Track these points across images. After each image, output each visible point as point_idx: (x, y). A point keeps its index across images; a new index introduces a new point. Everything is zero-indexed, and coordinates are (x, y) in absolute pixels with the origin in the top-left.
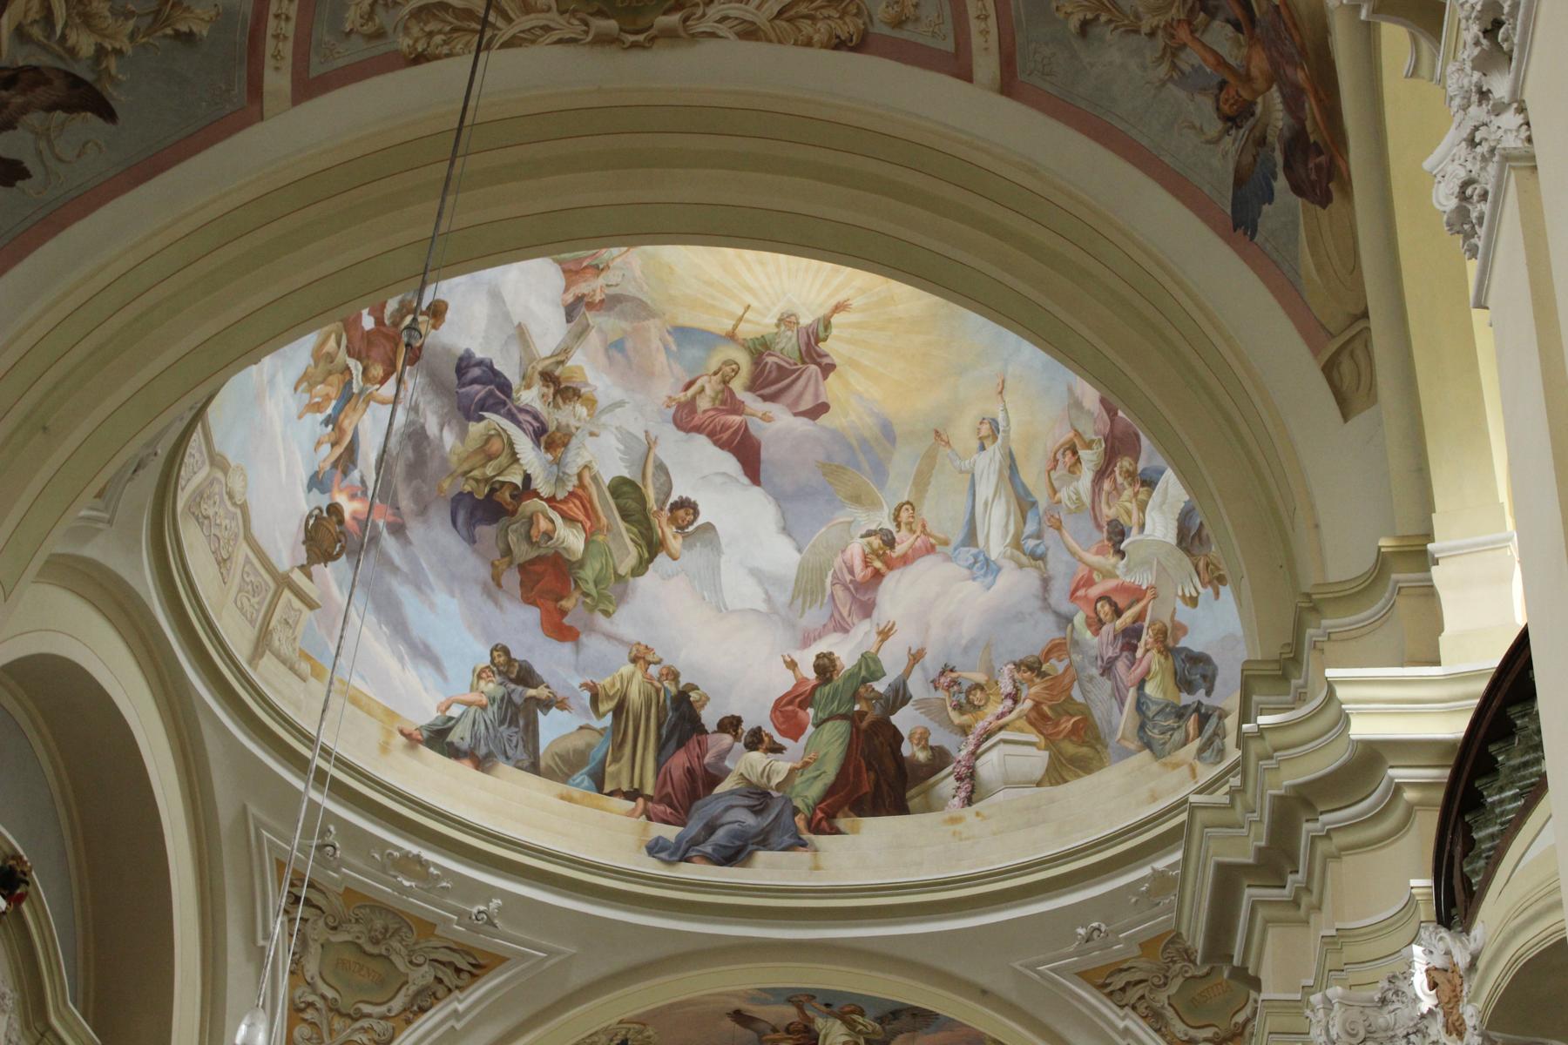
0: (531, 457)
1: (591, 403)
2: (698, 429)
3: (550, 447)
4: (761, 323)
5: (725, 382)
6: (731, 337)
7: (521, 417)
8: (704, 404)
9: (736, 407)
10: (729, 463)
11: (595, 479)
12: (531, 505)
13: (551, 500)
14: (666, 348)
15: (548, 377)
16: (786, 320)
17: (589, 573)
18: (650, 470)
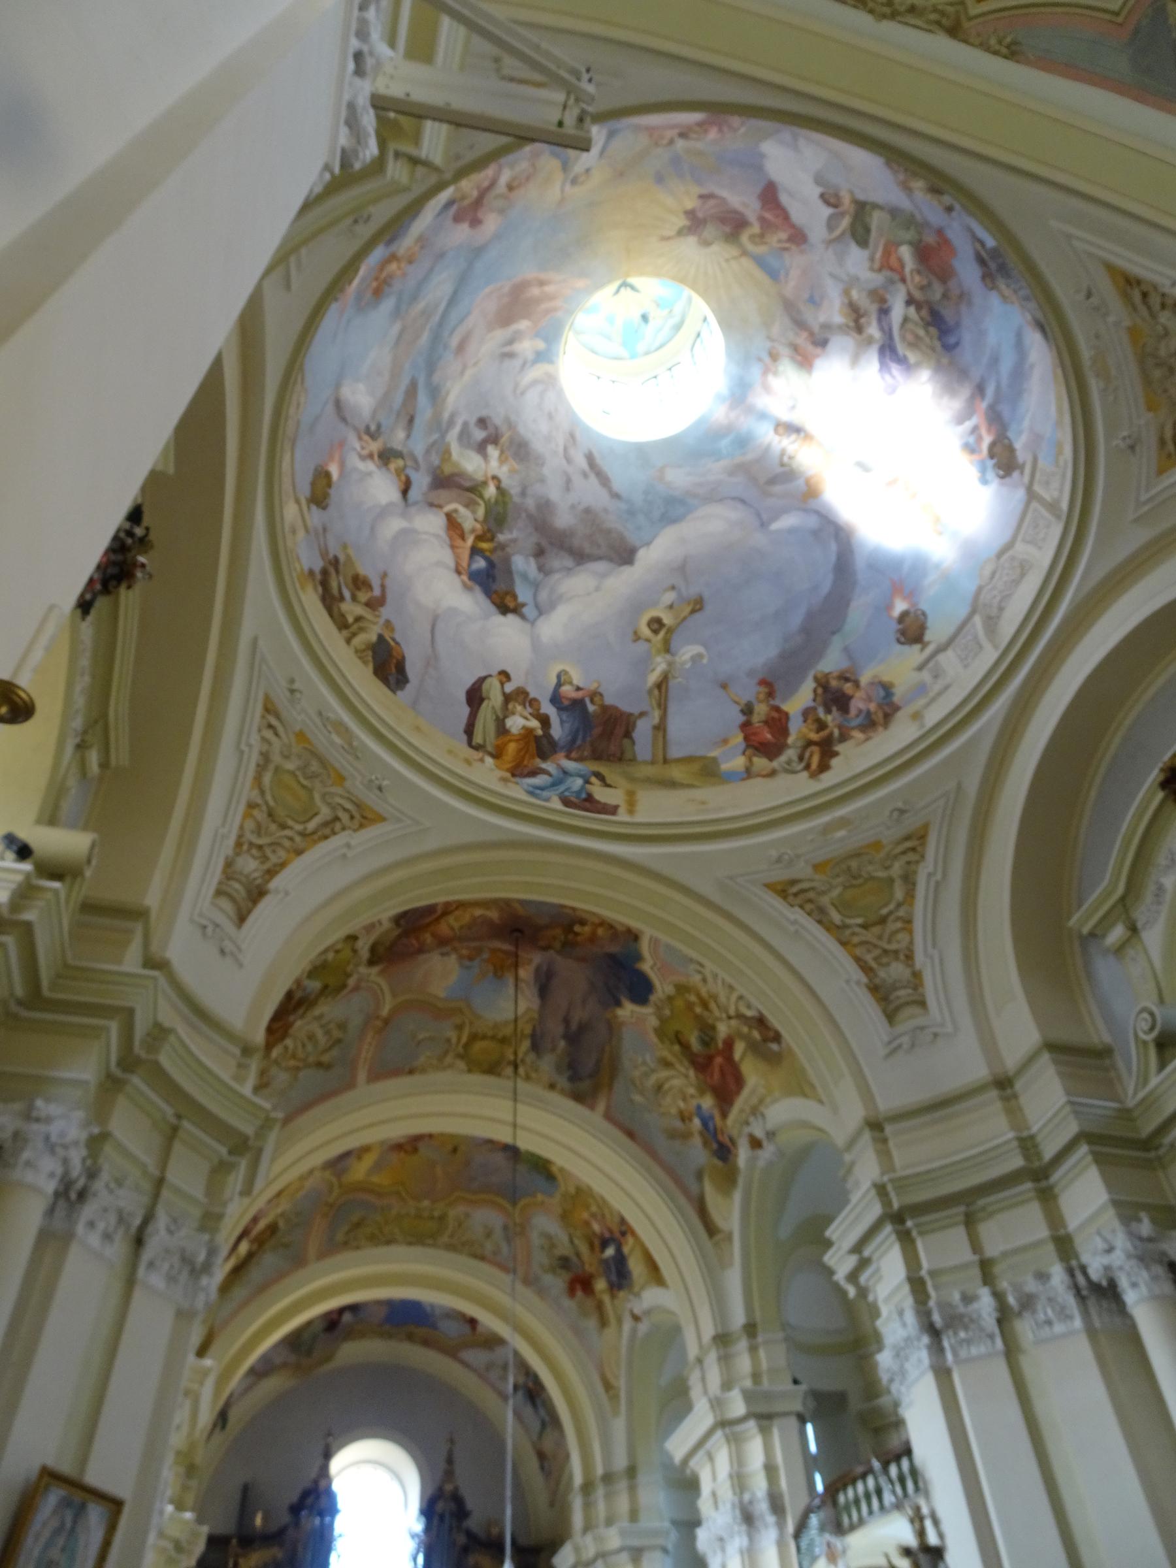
0: (898, 310)
1: (846, 292)
2: (793, 226)
3: (883, 300)
4: (720, 251)
5: (762, 236)
6: (745, 253)
7: (886, 328)
8: (783, 235)
9: (762, 220)
10: (784, 199)
11: (872, 259)
12: (918, 295)
13: (903, 280)
14: (787, 274)
15: (859, 329)
16: (706, 243)
17: (910, 235)
18: (837, 232)
